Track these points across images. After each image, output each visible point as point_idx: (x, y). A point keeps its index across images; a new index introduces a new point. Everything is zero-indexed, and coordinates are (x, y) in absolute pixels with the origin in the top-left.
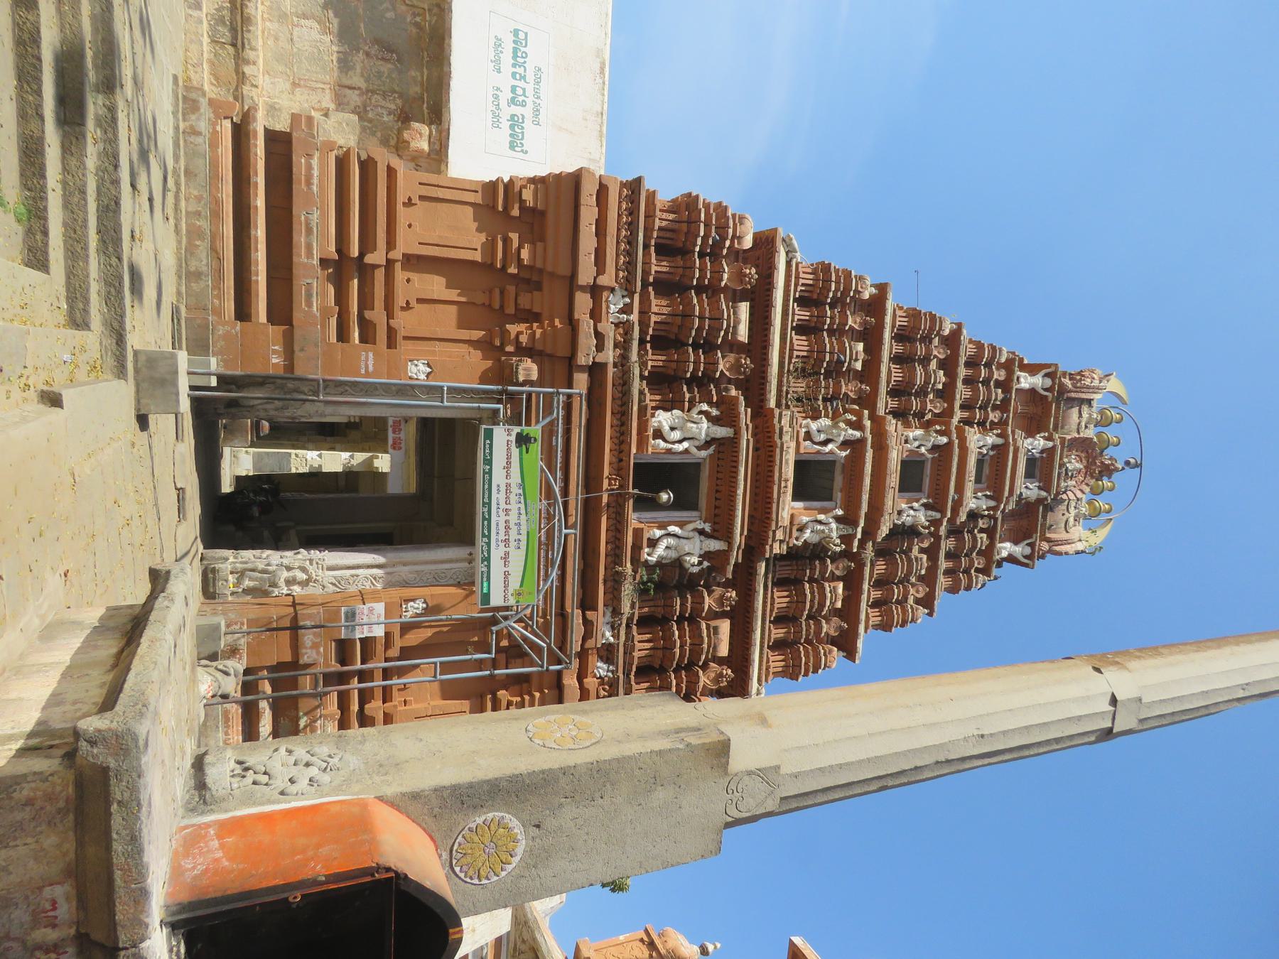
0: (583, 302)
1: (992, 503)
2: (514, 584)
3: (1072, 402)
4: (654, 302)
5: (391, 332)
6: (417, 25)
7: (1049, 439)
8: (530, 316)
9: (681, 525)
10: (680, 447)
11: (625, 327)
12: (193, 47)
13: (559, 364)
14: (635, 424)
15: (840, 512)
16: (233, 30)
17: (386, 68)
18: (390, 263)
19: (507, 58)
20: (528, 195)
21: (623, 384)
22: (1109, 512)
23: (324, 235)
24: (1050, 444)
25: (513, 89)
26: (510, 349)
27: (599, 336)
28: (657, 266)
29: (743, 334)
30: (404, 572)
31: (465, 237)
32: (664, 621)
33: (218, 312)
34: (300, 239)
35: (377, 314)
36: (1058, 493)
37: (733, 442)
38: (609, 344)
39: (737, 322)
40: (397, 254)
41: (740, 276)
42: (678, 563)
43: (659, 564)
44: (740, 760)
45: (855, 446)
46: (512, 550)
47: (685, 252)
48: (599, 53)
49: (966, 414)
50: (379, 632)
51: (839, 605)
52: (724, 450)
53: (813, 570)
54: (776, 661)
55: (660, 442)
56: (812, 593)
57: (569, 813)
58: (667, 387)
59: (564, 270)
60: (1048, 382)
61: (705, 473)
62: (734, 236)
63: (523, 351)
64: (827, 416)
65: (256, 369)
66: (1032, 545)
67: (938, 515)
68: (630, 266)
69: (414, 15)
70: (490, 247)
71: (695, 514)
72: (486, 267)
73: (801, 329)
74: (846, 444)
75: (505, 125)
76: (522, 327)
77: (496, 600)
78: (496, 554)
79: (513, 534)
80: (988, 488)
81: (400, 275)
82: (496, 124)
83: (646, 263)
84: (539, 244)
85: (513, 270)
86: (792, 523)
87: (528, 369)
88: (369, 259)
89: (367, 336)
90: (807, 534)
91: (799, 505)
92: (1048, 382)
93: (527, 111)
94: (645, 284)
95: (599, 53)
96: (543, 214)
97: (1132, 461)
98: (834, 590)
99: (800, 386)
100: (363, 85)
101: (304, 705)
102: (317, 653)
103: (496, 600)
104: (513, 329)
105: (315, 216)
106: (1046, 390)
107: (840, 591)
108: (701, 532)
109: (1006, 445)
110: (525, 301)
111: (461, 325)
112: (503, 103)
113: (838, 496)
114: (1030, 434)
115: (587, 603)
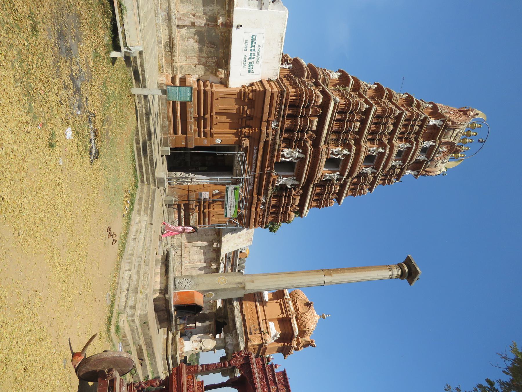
0: (264, 124)
1: (402, 164)
2: (232, 214)
3: (451, 129)
4: (286, 120)
6: (223, 36)
7: (434, 142)
8: (249, 127)
9: (287, 176)
10: (288, 160)
11: (276, 130)
12: (160, 55)
13: (255, 139)
14: (276, 155)
15: (338, 173)
16: (170, 47)
17: (212, 50)
18: (211, 116)
19: (249, 45)
20: (250, 96)
21: (274, 144)
22: (463, 157)
23: (194, 112)
25: (251, 54)
26: (243, 136)
29: (314, 127)
31: (232, 107)
32: (281, 197)
33: (170, 134)
34: (189, 115)
36: (433, 158)
37: (304, 159)
39: (312, 125)
40: (213, 114)
41: (315, 111)
44: (247, 288)
45: (347, 157)
46: (232, 208)
49: (401, 136)
52: (302, 161)
53: (329, 183)
54: (314, 204)
55: (283, 159)
56: (328, 189)
57: (220, 293)
59: (259, 116)
60: (441, 123)
61: (297, 165)
62: (315, 101)
63: (246, 137)
64: (341, 146)
65: (179, 146)
66: (418, 172)
67: (375, 171)
69: (221, 33)
70: (239, 109)
71: (292, 174)
72: (238, 113)
73: (338, 120)
74: (345, 155)
75: (247, 66)
76: (247, 130)
78: (228, 209)
79: (232, 205)
81: (214, 117)
82: (244, 66)
83: (284, 111)
84: (253, 109)
85: (245, 116)
86: (322, 176)
87: (246, 143)
88: (206, 116)
89: (205, 135)
90: (327, 177)
91: (327, 169)
92: (441, 123)
93: (255, 60)
95: (281, 35)
96: (254, 101)
97: (481, 140)
98: (336, 188)
99: (334, 136)
100: (206, 56)
101: (191, 211)
102: (193, 203)
104: (243, 130)
105: (192, 109)
106: (439, 125)
107: (338, 188)
109: (412, 148)
110: (248, 123)
111: (230, 129)
112: (247, 59)
113: (340, 167)
115: (259, 194)
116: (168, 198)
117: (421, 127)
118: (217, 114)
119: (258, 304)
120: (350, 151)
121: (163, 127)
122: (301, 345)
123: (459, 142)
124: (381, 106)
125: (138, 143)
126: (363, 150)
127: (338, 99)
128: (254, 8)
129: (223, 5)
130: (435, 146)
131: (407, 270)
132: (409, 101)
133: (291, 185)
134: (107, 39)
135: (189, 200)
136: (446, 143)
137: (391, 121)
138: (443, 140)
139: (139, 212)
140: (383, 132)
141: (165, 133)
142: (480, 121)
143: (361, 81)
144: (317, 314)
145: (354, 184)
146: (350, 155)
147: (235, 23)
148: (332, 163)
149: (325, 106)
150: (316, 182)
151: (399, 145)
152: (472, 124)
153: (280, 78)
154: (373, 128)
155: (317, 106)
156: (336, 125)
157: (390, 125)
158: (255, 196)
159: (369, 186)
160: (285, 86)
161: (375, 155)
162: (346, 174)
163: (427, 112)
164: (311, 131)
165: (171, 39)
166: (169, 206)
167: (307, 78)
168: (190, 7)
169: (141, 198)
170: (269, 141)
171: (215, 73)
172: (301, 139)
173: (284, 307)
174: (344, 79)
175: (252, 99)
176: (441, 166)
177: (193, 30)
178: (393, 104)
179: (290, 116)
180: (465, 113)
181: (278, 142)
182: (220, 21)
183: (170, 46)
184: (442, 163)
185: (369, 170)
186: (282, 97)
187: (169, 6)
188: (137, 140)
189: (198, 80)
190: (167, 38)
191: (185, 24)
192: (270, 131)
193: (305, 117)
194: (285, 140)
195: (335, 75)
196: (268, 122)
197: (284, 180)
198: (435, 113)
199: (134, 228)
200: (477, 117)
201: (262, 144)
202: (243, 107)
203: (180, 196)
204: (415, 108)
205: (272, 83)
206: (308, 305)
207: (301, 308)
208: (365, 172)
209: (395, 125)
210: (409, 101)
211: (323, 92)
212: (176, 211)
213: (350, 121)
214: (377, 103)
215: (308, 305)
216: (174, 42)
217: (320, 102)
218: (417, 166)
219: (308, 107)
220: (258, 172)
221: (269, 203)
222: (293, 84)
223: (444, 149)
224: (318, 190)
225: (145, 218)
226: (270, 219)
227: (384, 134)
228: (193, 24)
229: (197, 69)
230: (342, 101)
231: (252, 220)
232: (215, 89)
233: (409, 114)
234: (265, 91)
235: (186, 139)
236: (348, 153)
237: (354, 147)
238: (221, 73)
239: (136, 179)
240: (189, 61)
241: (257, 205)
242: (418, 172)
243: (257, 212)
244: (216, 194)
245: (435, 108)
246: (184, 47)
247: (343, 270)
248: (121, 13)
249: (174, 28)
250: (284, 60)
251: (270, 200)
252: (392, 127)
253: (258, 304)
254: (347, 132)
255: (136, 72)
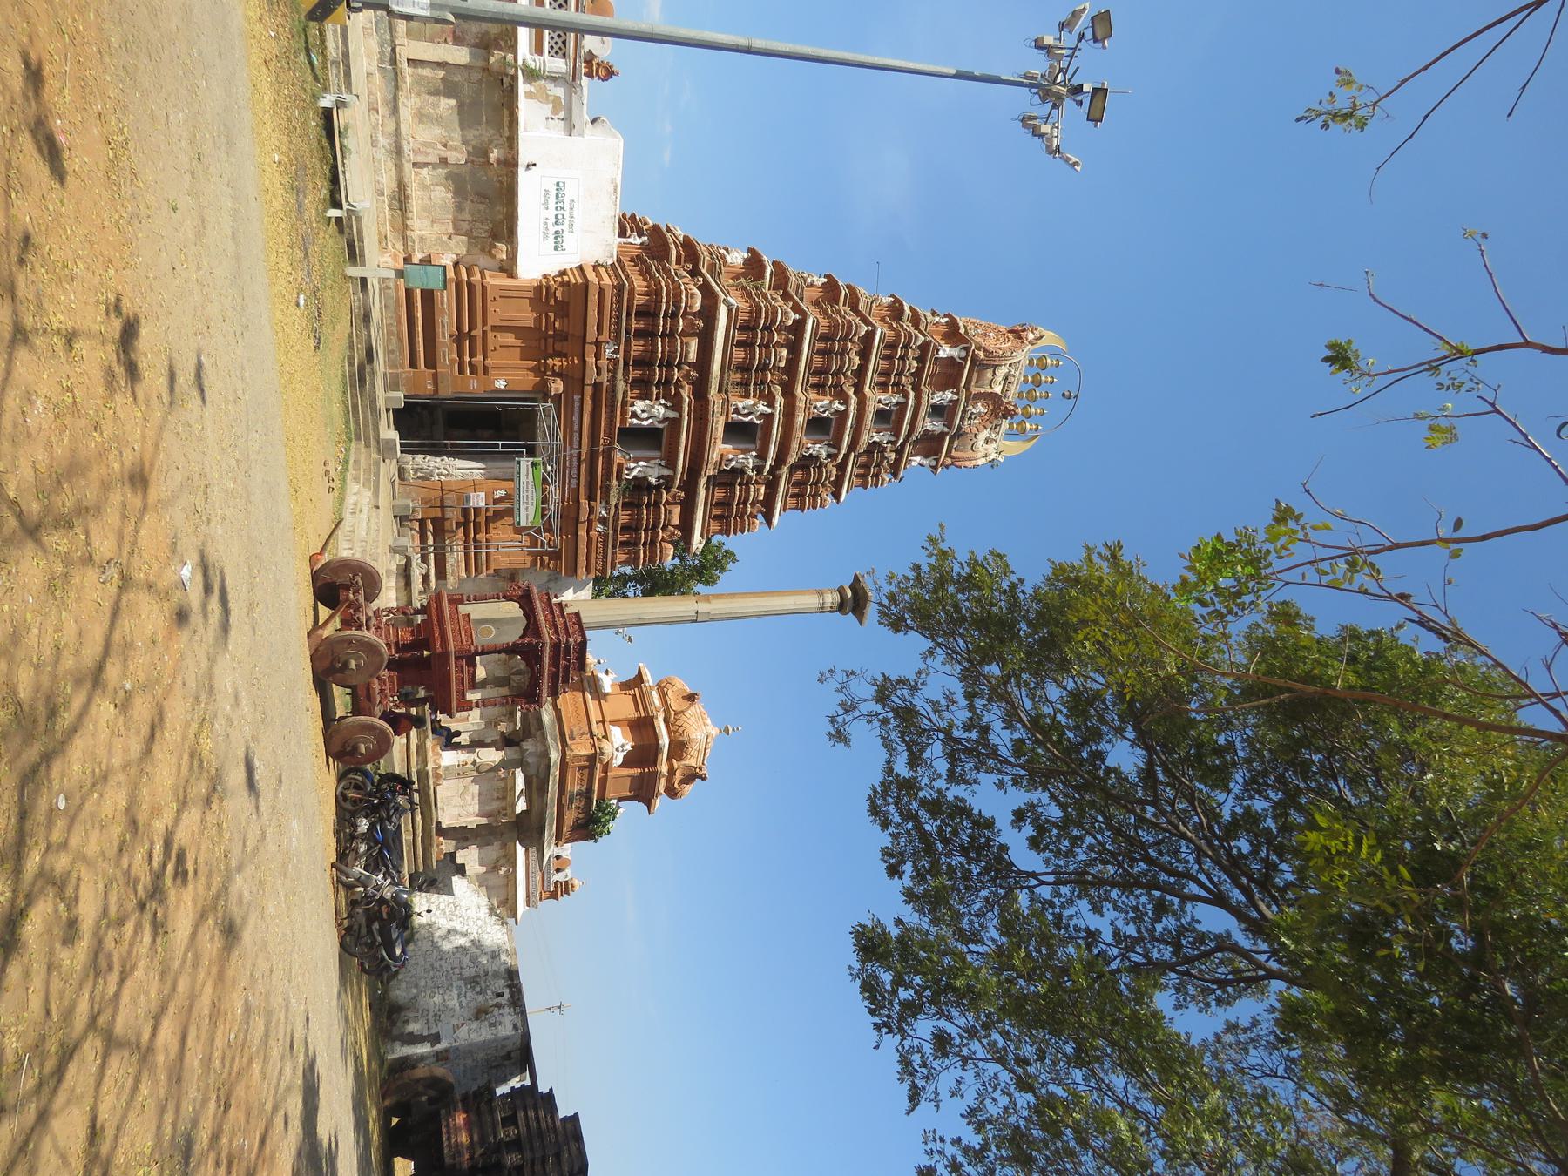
2: (531, 518)
3: (987, 366)
7: (957, 393)
9: (647, 460)
10: (645, 423)
13: (575, 380)
17: (482, 207)
18: (484, 332)
20: (559, 294)
21: (613, 390)
29: (692, 357)
30: (497, 472)
32: (639, 506)
33: (402, 366)
34: (439, 330)
36: (960, 428)
40: (488, 328)
42: (645, 478)
45: (768, 418)
47: (655, 315)
48: (613, 181)
50: (482, 504)
54: (715, 526)
55: (635, 421)
58: (643, 388)
59: (579, 333)
60: (963, 354)
63: (555, 374)
65: (420, 393)
68: (618, 331)
71: (656, 454)
72: (537, 328)
73: (740, 344)
74: (762, 415)
75: (551, 238)
77: (523, 524)
81: (491, 335)
82: (546, 237)
87: (557, 386)
92: (963, 354)
93: (565, 227)
95: (613, 181)
98: (757, 491)
99: (738, 378)
101: (447, 535)
102: (453, 515)
103: (523, 524)
109: (906, 404)
110: (558, 346)
114: (943, 388)
115: (591, 497)
116: (399, 502)
117: (921, 360)
118: (494, 328)
119: (588, 696)
120: (771, 404)
121: (389, 352)
122: (678, 777)
123: (1020, 396)
124: (829, 317)
125: (351, 364)
126: (801, 404)
127: (732, 301)
128: (556, 131)
129: (499, 127)
130: (956, 403)
131: (849, 594)
132: (896, 310)
133: (659, 478)
134: (325, 192)
135: (442, 507)
136: (980, 396)
138: (974, 390)
139: (356, 479)
140: (838, 372)
141: (391, 364)
142: (1056, 354)
143: (791, 270)
144: (715, 724)
145: (797, 484)
146: (772, 415)
147: (523, 159)
148: (738, 431)
149: (708, 313)
150: (710, 472)
151: (877, 399)
152: (1040, 359)
153: (619, 261)
154: (818, 361)
155: (694, 314)
156: (738, 354)
157: (852, 355)
158: (584, 502)
159: (831, 489)
160: (627, 277)
161: (827, 419)
162: (772, 454)
163: (938, 333)
164: (689, 364)
165: (402, 187)
166: (402, 519)
167: (678, 262)
168: (437, 131)
169: (357, 462)
171: (489, 251)
172: (668, 382)
173: (641, 701)
174: (754, 264)
175: (563, 301)
176: (989, 446)
177: (442, 171)
178: (858, 313)
179: (640, 334)
180: (1018, 334)
181: (621, 385)
182: (494, 155)
183: (401, 200)
184: (987, 442)
185: (820, 450)
186: (620, 295)
187: (398, 129)
188: (351, 358)
189: (456, 265)
190: (394, 185)
191: (428, 160)
192: (603, 362)
193: (670, 335)
194: (635, 383)
195: (737, 258)
196: (598, 344)
197: (639, 466)
198: (953, 334)
199: (350, 500)
200: (1041, 343)
201: (588, 391)
203: (425, 501)
204: (907, 324)
205: (602, 270)
206: (691, 698)
207: (675, 704)
209: (864, 354)
210: (896, 310)
211: (706, 289)
212: (417, 536)
213: (767, 346)
214: (825, 314)
215: (691, 698)
216: (409, 191)
217: (698, 305)
218: (930, 445)
219: (674, 316)
220: (585, 449)
221: (616, 520)
222: (646, 272)
223: (980, 408)
224: (719, 494)
225: (366, 496)
226: (621, 556)
228: (444, 161)
229: (453, 243)
230: (744, 306)
231: (582, 558)
232: (489, 281)
233: (892, 334)
234: (586, 284)
235: (435, 377)
237: (779, 399)
238: (501, 251)
239: (348, 427)
240: (436, 228)
241: (590, 521)
242: (937, 460)
243: (589, 539)
244: (501, 500)
245: (953, 324)
246: (426, 201)
247: (733, 595)
248: (343, 157)
249: (408, 167)
250: (627, 225)
251: (616, 514)
252: (857, 360)
253: (588, 696)
254: (763, 368)
255: (351, 246)
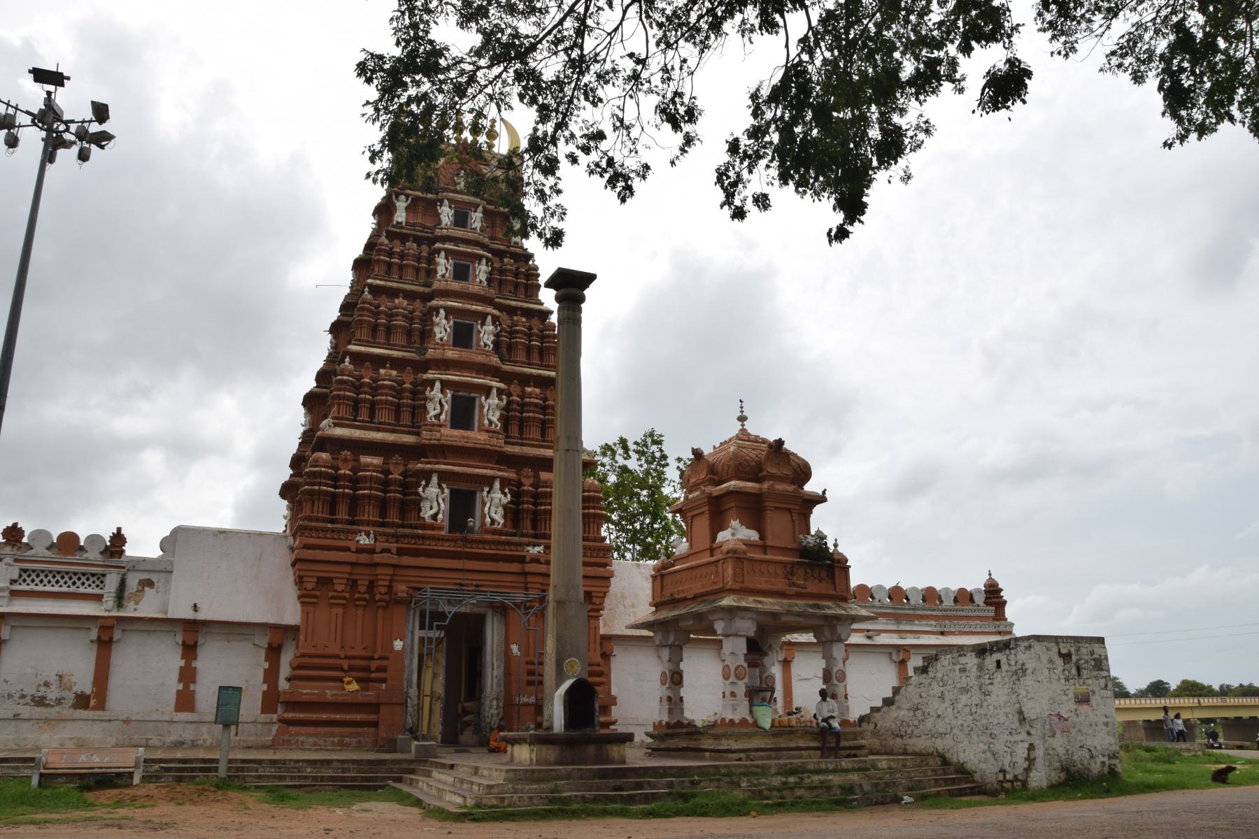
1: (484, 261)
5: (382, 658)
9: (484, 504)
18: (347, 657)
24: (446, 202)
27: (383, 551)
28: (342, 514)
35: (374, 665)
38: (387, 545)
39: (375, 466)
42: (505, 507)
43: (505, 517)
47: (334, 496)
51: (538, 390)
59: (348, 569)
60: (403, 197)
67: (489, 317)
74: (442, 391)
80: (473, 263)
88: (346, 667)
92: (403, 197)
94: (352, 523)
108: (489, 492)
110: (362, 589)
137: (385, 304)
146: (442, 382)
147: (187, 614)
170: (398, 549)
202: (332, 598)
208: (492, 338)
227: (411, 313)
236: (438, 385)
